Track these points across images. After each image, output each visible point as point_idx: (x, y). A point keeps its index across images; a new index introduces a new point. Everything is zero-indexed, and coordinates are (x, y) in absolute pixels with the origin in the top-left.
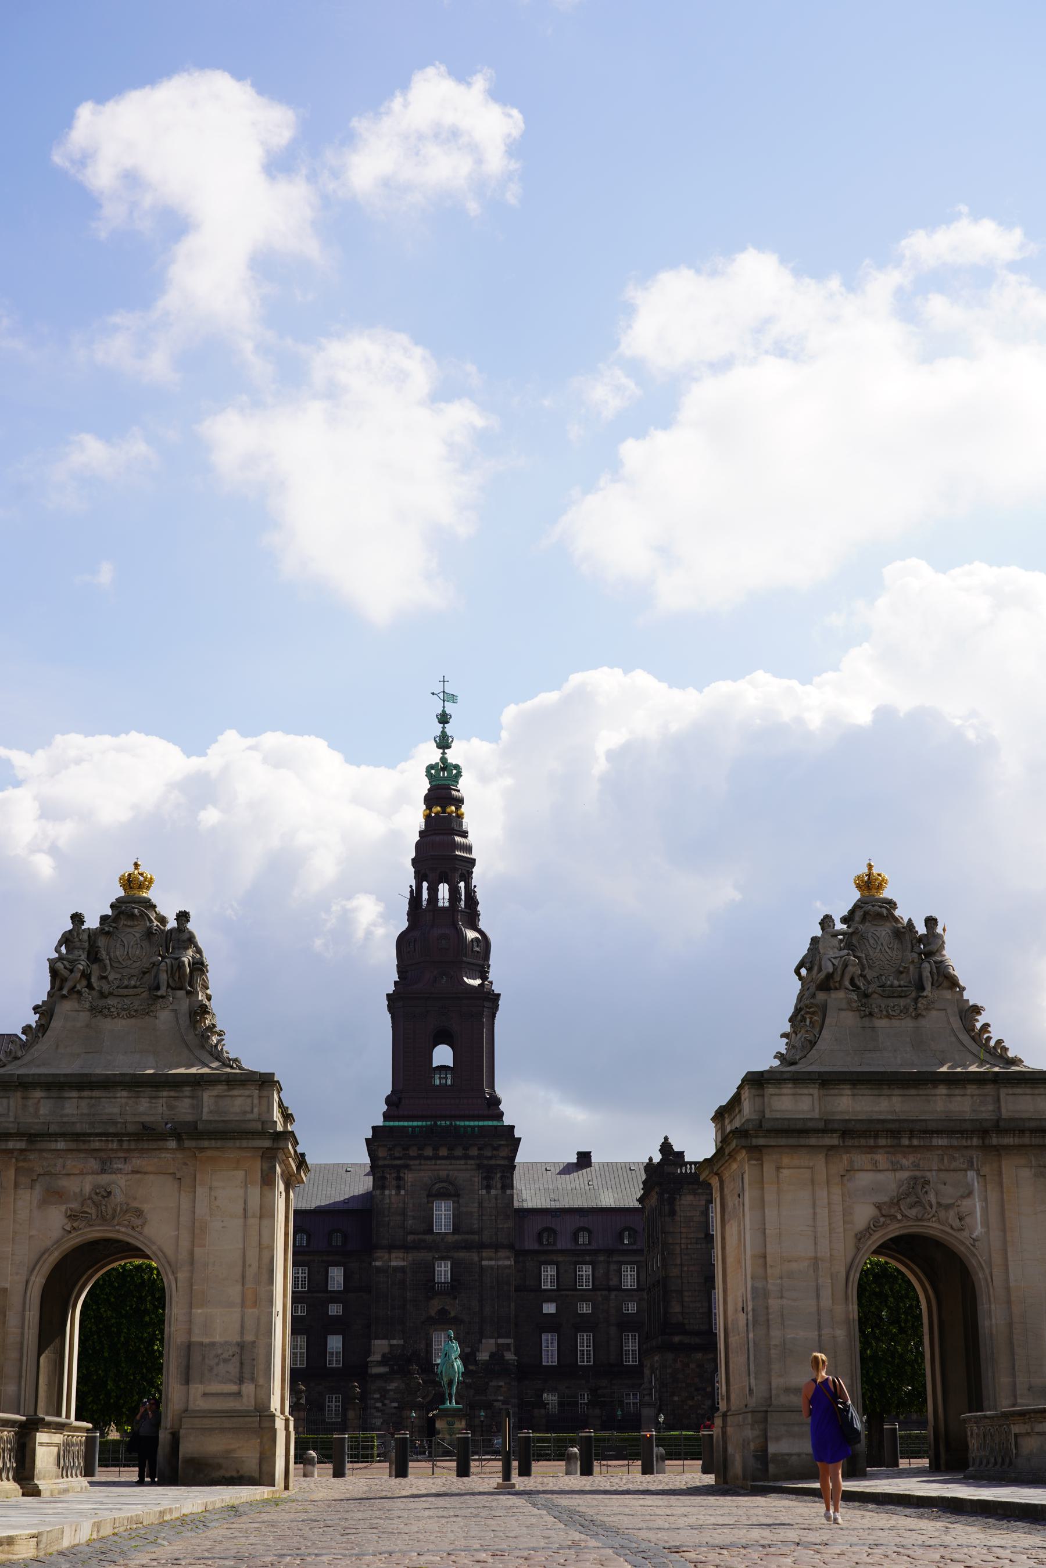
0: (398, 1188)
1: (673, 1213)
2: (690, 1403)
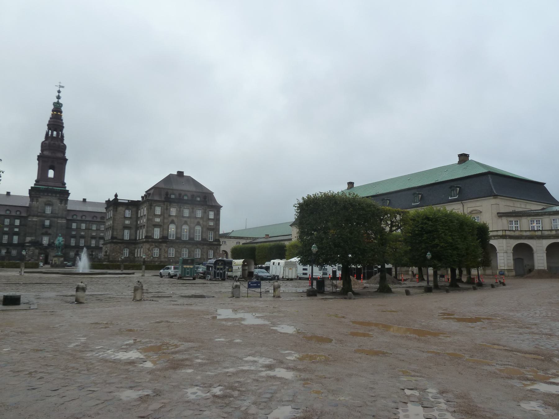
0: (37, 202)
1: (116, 211)
2: (117, 255)
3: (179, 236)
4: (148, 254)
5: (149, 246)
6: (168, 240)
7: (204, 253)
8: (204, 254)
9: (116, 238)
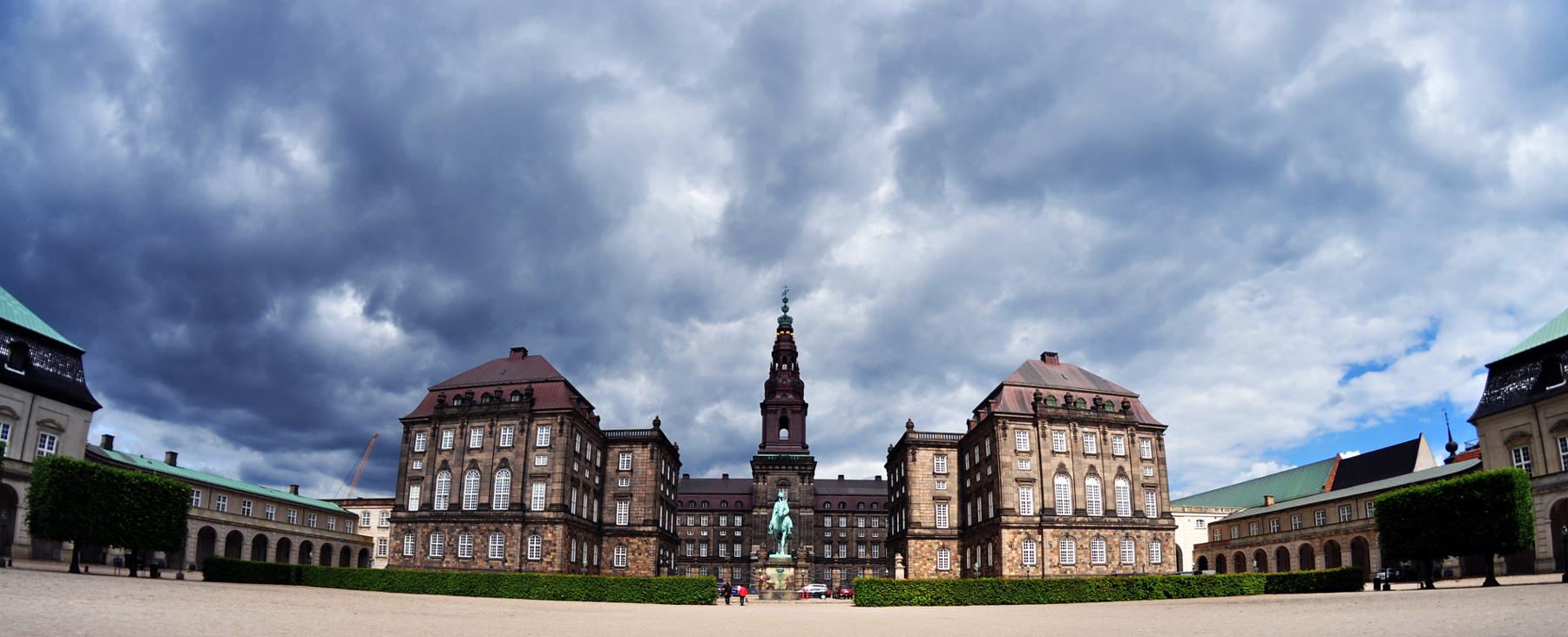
0: (764, 482)
1: (914, 460)
3: (1080, 506)
4: (1010, 558)
5: (1012, 536)
6: (1056, 518)
7: (1143, 549)
8: (1142, 551)
9: (918, 525)
